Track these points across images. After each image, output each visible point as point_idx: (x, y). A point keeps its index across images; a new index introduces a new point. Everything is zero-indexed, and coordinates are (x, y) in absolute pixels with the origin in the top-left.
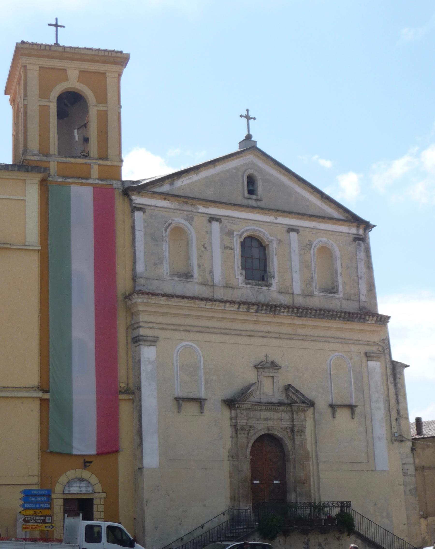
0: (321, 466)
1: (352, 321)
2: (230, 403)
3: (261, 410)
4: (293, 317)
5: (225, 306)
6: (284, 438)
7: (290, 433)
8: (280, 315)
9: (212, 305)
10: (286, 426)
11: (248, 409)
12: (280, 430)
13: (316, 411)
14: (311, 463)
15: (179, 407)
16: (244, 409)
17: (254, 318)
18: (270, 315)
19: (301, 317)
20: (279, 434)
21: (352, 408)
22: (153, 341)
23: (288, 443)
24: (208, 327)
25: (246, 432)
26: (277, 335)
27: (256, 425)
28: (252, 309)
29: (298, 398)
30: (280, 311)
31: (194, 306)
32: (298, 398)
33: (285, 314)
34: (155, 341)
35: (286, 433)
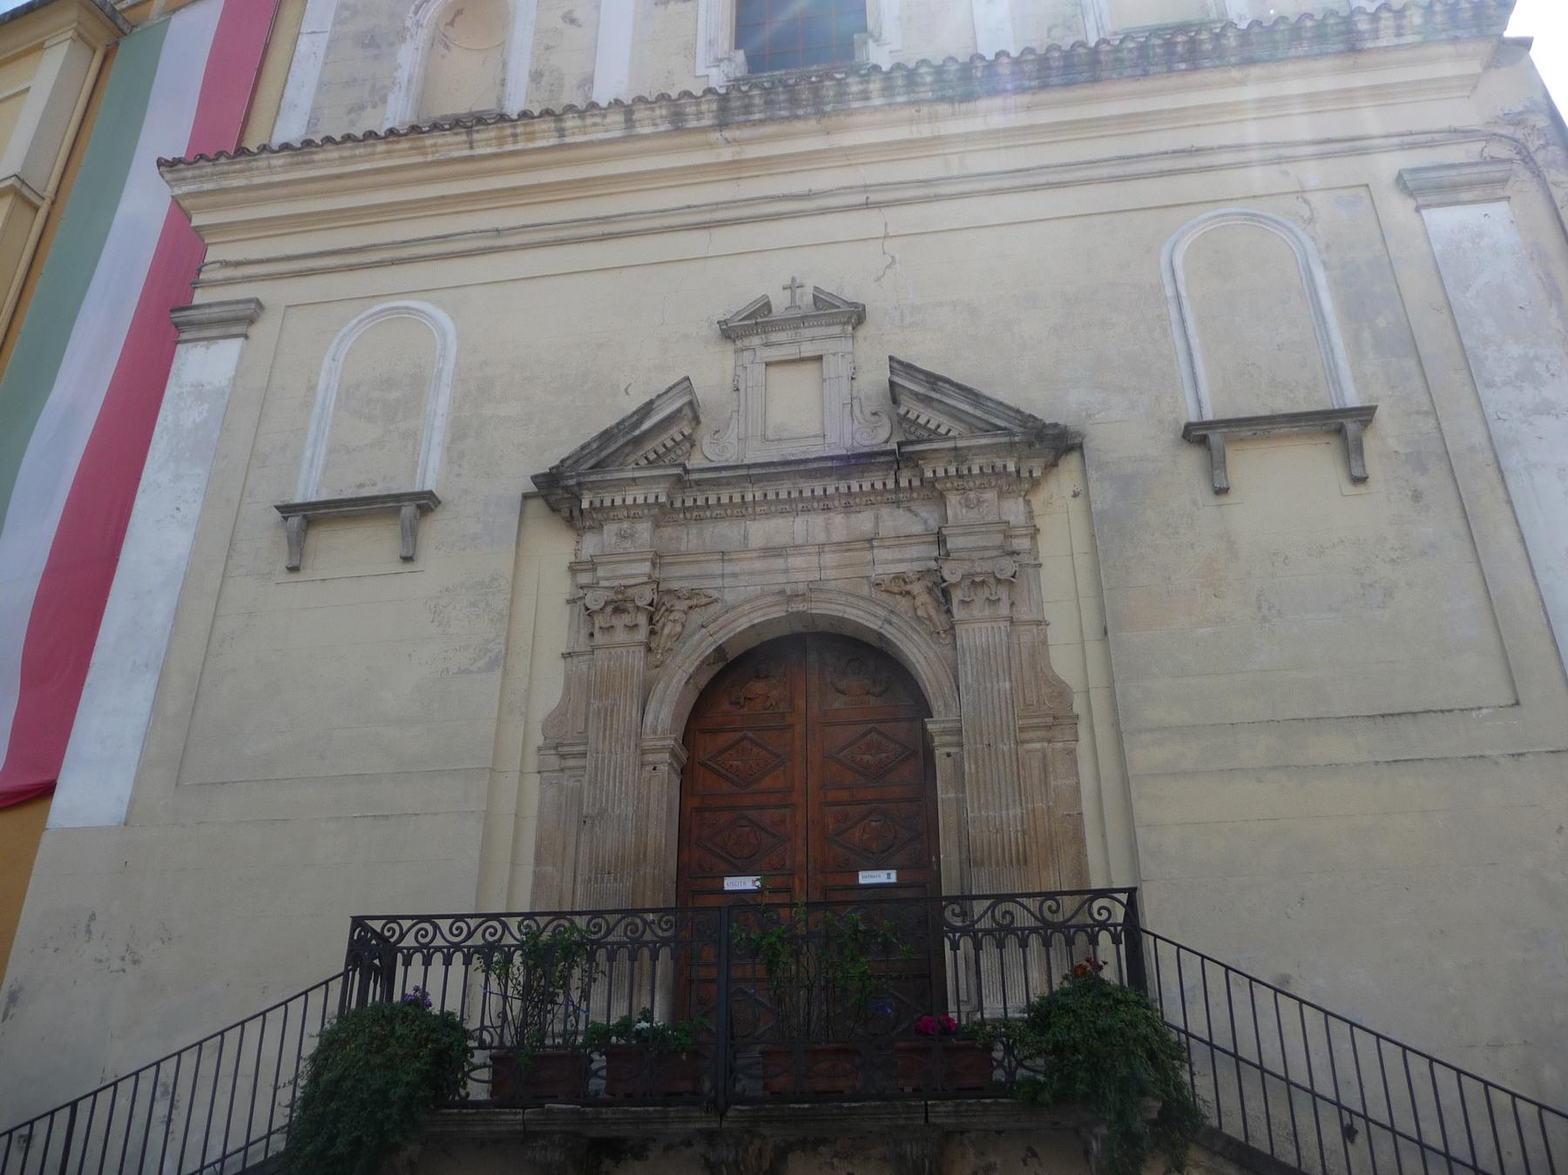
0: (1143, 757)
1: (1272, 59)
2: (560, 493)
3: (742, 511)
4: (925, 110)
5: (561, 132)
6: (890, 632)
7: (923, 598)
8: (851, 113)
9: (501, 140)
10: (901, 568)
11: (663, 514)
12: (865, 590)
13: (1093, 475)
14: (1083, 748)
15: (298, 544)
16: (632, 513)
17: (727, 154)
18: (799, 125)
19: (967, 97)
20: (865, 615)
21: (1342, 427)
22: (240, 320)
23: (918, 653)
24: (498, 232)
25: (642, 619)
26: (861, 199)
27: (718, 583)
28: (699, 115)
29: (956, 414)
30: (841, 95)
31: (420, 159)
32: (956, 414)
33: (877, 101)
34: (251, 321)
35: (903, 603)
